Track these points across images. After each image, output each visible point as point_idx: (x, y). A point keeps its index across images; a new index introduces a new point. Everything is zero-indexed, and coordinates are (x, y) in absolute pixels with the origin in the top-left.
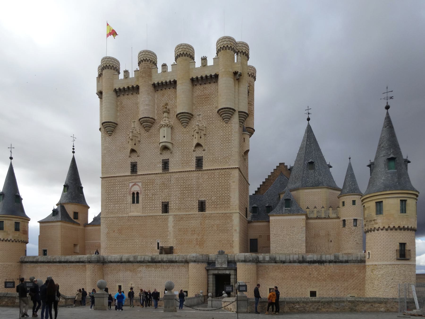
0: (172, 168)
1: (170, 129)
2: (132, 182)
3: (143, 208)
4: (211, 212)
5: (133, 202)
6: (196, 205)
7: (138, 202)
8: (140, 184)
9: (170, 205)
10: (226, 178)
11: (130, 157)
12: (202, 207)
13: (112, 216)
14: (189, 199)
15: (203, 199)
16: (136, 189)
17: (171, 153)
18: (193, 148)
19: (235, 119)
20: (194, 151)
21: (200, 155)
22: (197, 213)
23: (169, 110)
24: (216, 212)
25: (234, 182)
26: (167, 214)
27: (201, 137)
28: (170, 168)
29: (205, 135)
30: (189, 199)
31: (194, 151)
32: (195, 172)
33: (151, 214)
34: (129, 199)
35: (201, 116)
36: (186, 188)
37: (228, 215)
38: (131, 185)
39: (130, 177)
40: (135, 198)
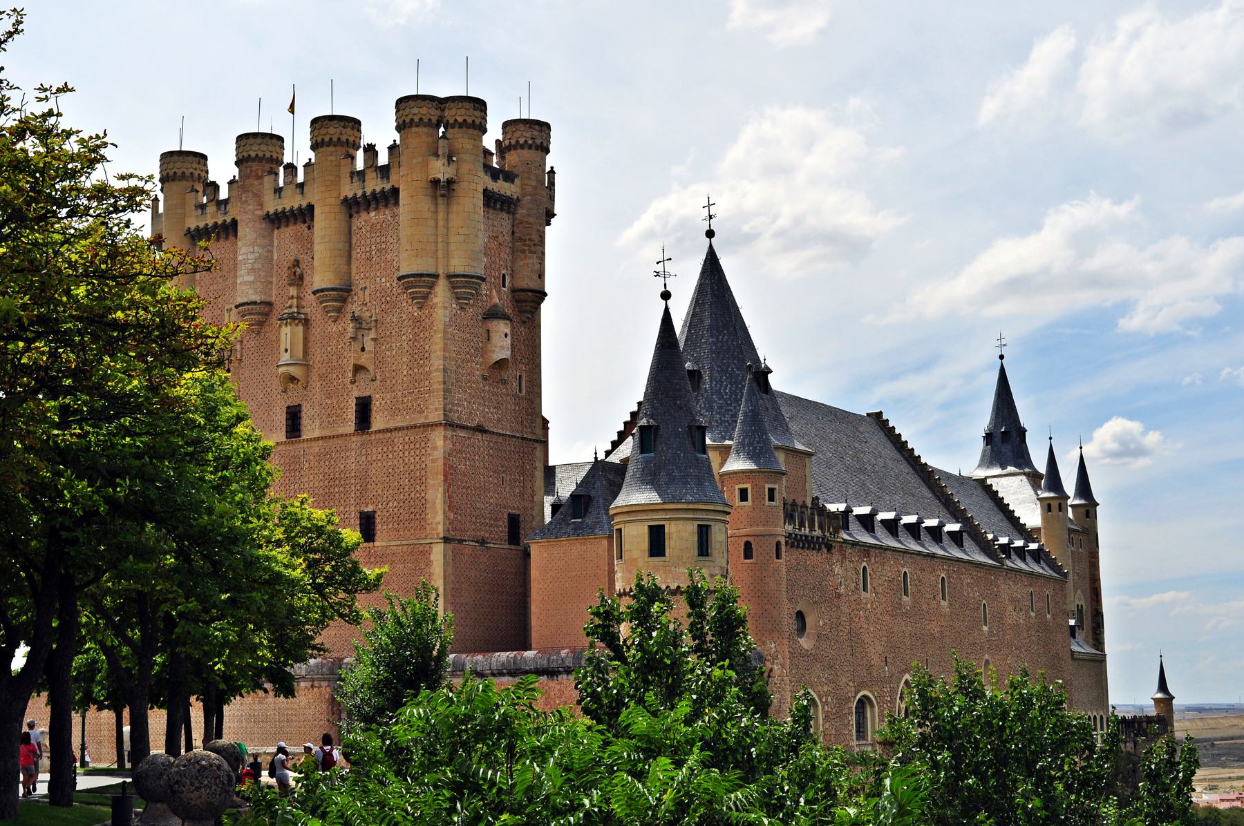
1: (300, 328)
15: (370, 509)
17: (305, 388)
18: (350, 375)
19: (441, 292)
20: (352, 382)
21: (367, 394)
23: (301, 278)
27: (363, 349)
28: (302, 428)
29: (374, 340)
31: (352, 382)
32: (354, 439)
35: (367, 292)
36: (334, 480)
37: (421, 548)
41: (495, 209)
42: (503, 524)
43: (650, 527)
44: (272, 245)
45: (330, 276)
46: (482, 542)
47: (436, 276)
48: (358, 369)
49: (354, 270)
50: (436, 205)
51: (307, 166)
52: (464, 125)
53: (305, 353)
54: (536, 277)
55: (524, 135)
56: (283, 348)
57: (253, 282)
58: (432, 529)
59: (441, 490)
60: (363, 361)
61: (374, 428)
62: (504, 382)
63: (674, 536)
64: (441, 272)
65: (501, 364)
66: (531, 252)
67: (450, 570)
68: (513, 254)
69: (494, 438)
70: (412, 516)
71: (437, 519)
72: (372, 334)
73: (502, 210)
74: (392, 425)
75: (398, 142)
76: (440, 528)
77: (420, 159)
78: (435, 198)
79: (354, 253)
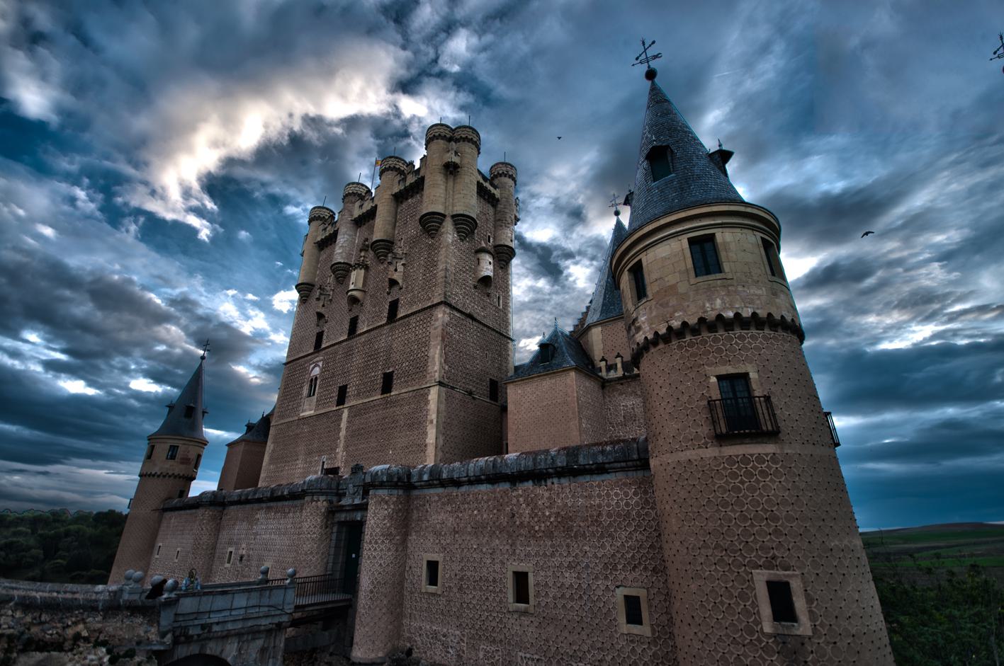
0: (363, 328)
1: (363, 271)
2: (314, 363)
3: (317, 401)
5: (309, 395)
7: (314, 394)
8: (321, 364)
9: (348, 390)
10: (425, 325)
11: (318, 325)
13: (282, 421)
14: (373, 374)
15: (391, 370)
16: (317, 371)
19: (448, 227)
20: (388, 293)
26: (341, 407)
27: (396, 270)
30: (373, 374)
39: (313, 356)
41: (484, 199)
42: (486, 383)
43: (691, 241)
44: (356, 236)
45: (382, 234)
46: (470, 393)
47: (444, 216)
48: (393, 283)
49: (396, 232)
50: (447, 179)
52: (466, 139)
53: (364, 285)
54: (509, 240)
55: (502, 169)
56: (351, 283)
57: (341, 253)
58: (431, 377)
59: (439, 347)
60: (396, 276)
61: (398, 317)
62: (488, 295)
63: (733, 246)
64: (447, 214)
65: (486, 281)
66: (506, 226)
67: (443, 407)
68: (495, 228)
69: (481, 327)
70: (418, 370)
71: (436, 367)
72: (403, 262)
73: (489, 202)
74: (410, 312)
75: (426, 154)
76: (437, 375)
77: (438, 155)
78: (446, 176)
79: (397, 224)
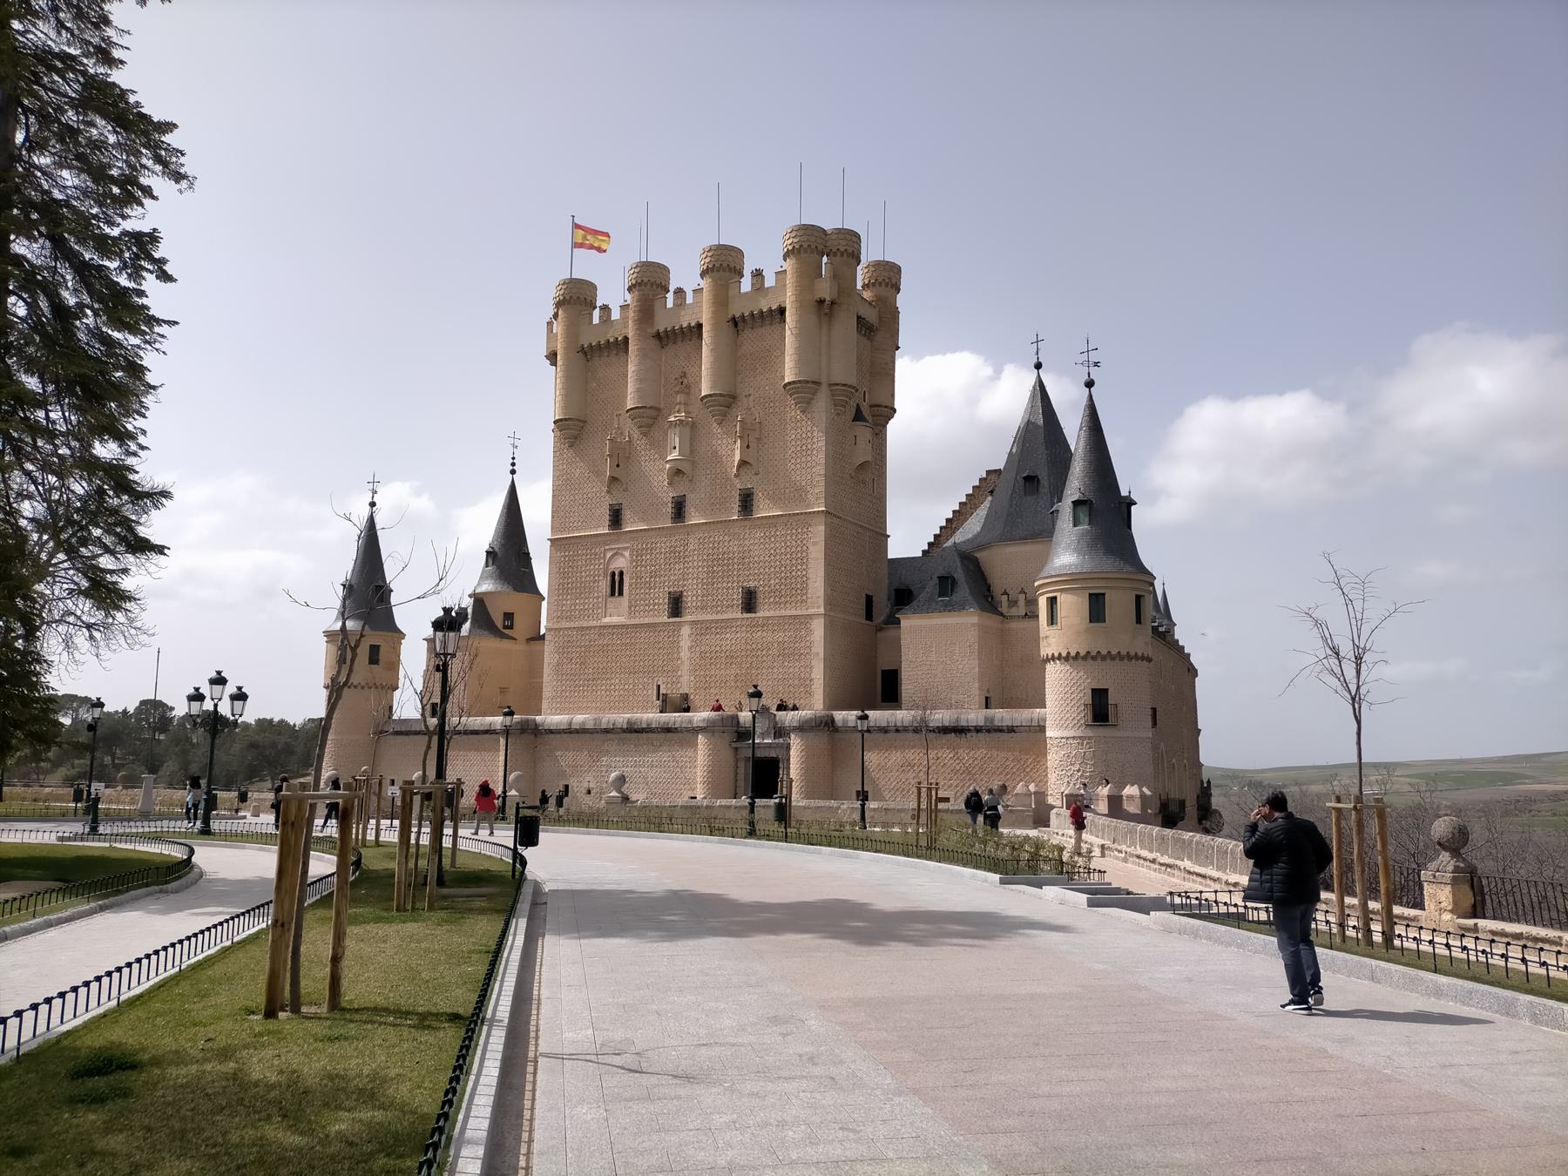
1: (688, 430)
4: (767, 614)
5: (613, 594)
6: (737, 598)
7: (621, 594)
8: (627, 554)
12: (750, 602)
13: (568, 625)
15: (752, 584)
22: (739, 615)
24: (778, 613)
25: (815, 544)
33: (646, 621)
34: (604, 585)
38: (609, 555)
40: (616, 585)
47: (818, 383)
51: (697, 291)
64: (824, 380)
65: (864, 466)
